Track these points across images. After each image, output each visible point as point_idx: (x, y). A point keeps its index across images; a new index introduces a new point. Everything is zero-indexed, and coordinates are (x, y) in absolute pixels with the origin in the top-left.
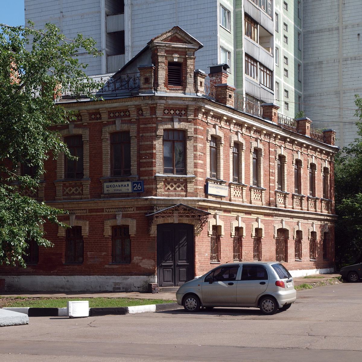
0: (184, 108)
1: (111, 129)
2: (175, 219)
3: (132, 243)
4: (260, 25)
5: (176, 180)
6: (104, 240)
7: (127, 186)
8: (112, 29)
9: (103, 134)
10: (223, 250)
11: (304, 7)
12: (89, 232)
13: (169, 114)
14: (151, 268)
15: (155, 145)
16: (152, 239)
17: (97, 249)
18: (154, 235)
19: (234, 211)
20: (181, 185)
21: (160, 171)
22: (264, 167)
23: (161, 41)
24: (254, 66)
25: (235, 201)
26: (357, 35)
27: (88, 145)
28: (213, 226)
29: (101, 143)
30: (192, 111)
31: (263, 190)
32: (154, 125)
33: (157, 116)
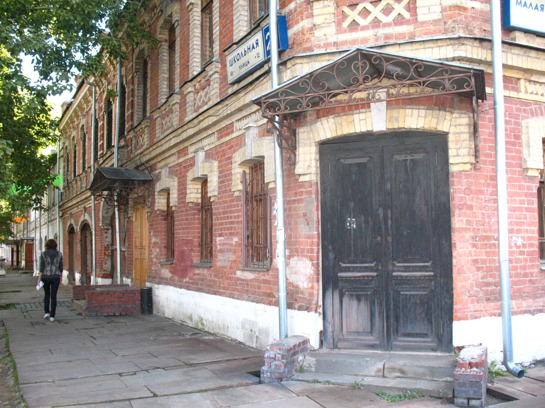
7: (255, 45)
12: (219, 188)
17: (228, 229)
20: (396, 5)
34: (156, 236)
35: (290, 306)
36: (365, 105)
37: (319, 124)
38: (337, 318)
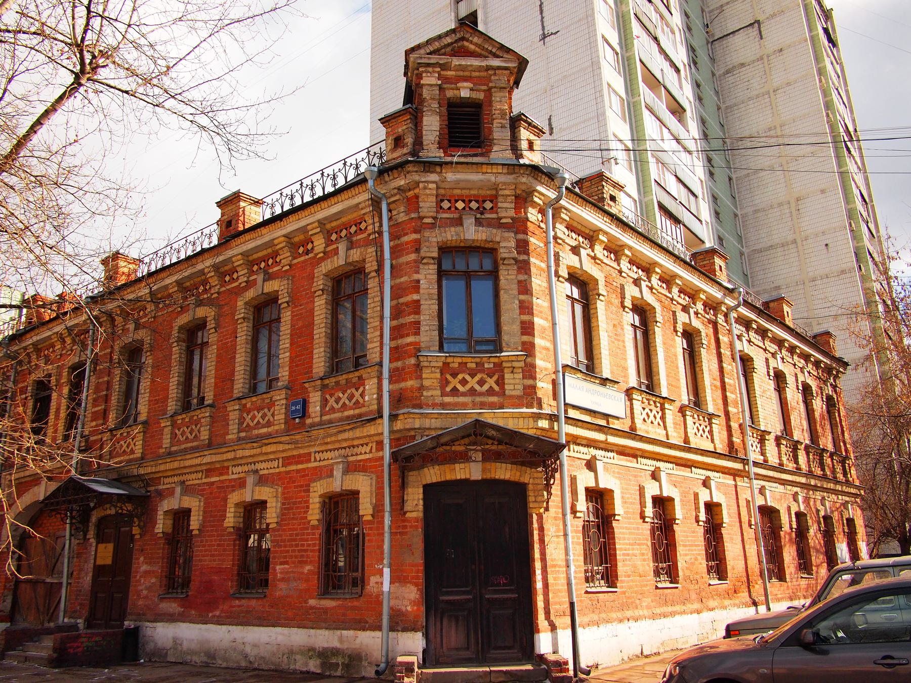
0: (491, 196)
1: (330, 267)
3: (367, 538)
4: (684, 225)
5: (474, 365)
6: (308, 534)
9: (315, 280)
10: (624, 554)
13: (453, 209)
14: (409, 608)
15: (418, 281)
16: (411, 527)
17: (296, 557)
18: (414, 515)
19: (646, 455)
20: (488, 379)
21: (431, 344)
23: (428, 54)
26: (824, 247)
27: (289, 313)
29: (314, 302)
30: (509, 199)
31: (711, 416)
32: (414, 236)
33: (421, 214)
34: (149, 563)
35: (392, 629)
36: (464, 457)
37: (426, 469)
38: (438, 636)
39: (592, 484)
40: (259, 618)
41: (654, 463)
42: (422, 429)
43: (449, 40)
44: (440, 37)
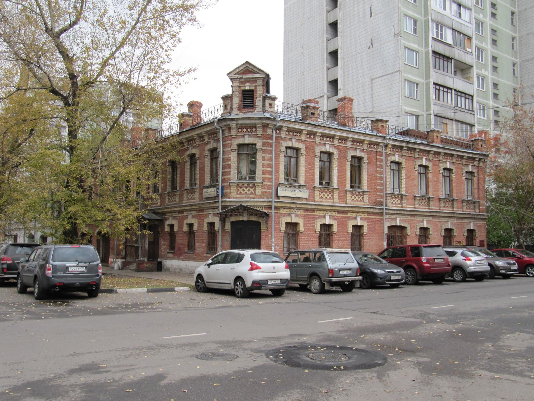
2: (245, 218)
8: (331, 79)
11: (519, 41)
22: (368, 173)
24: (447, 92)
25: (322, 202)
28: (286, 223)
31: (364, 192)
32: (230, 142)
39: (289, 221)
40: (193, 259)
41: (324, 212)
42: (230, 206)
43: (242, 68)
44: (238, 68)
